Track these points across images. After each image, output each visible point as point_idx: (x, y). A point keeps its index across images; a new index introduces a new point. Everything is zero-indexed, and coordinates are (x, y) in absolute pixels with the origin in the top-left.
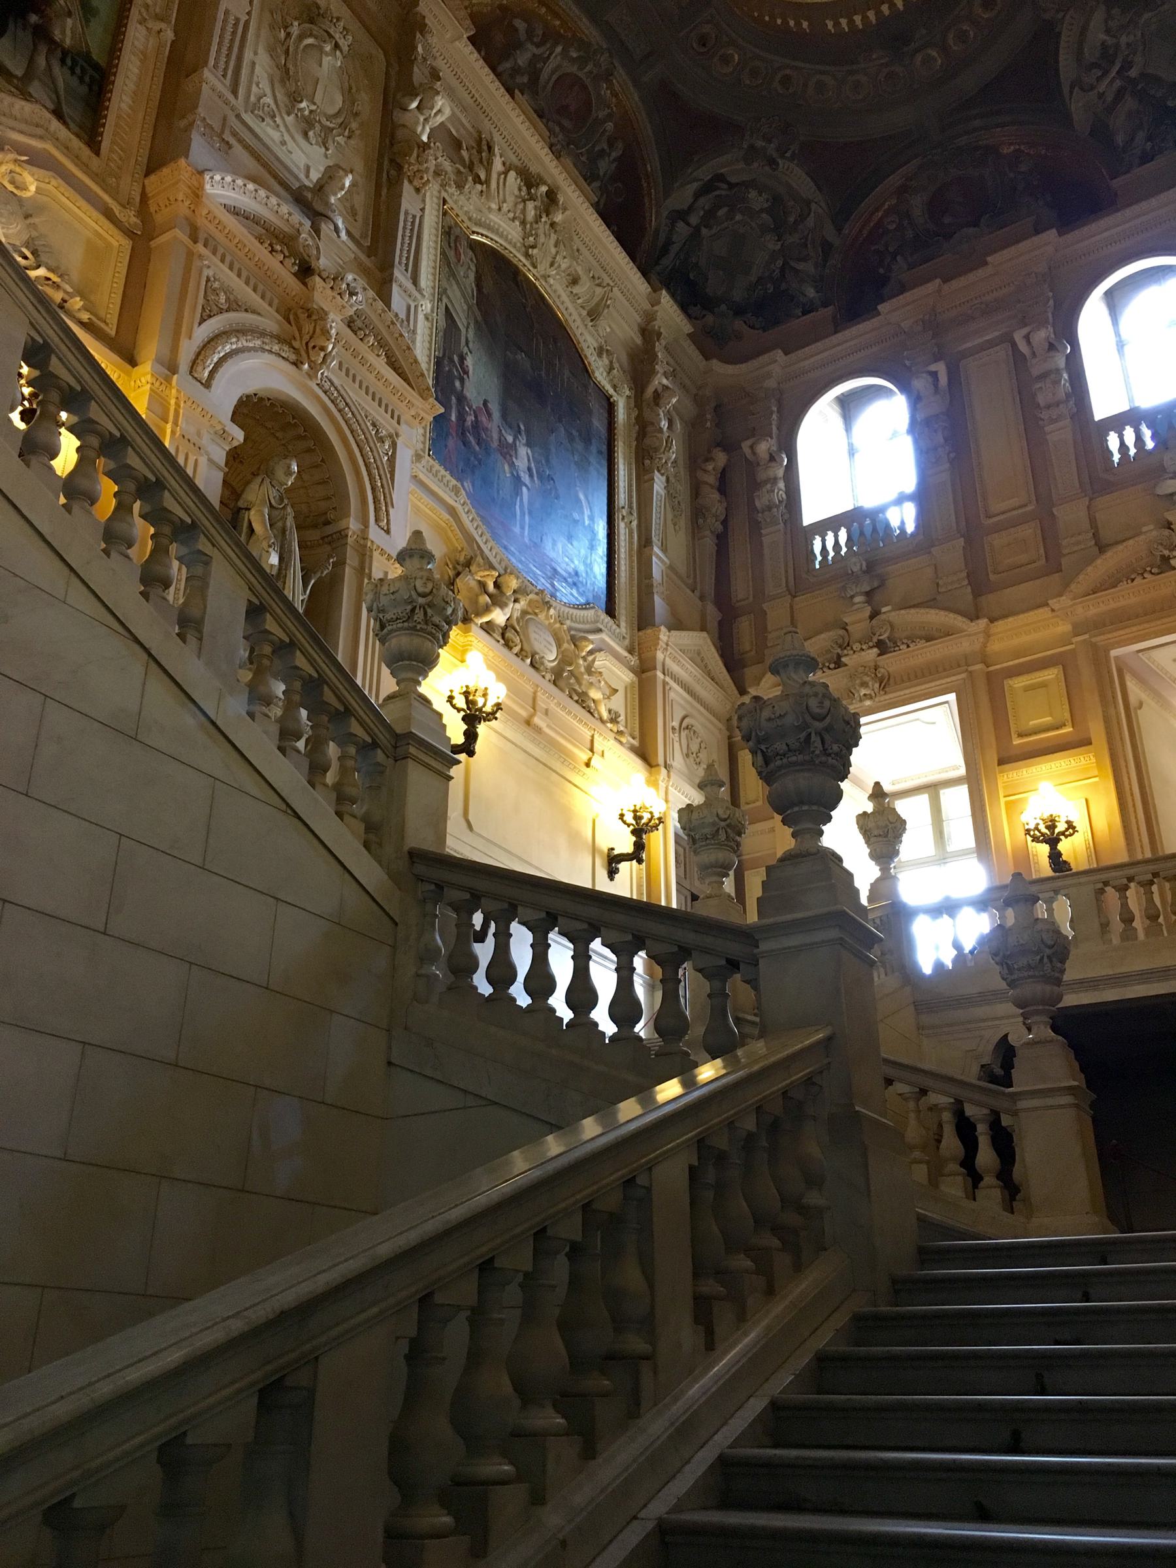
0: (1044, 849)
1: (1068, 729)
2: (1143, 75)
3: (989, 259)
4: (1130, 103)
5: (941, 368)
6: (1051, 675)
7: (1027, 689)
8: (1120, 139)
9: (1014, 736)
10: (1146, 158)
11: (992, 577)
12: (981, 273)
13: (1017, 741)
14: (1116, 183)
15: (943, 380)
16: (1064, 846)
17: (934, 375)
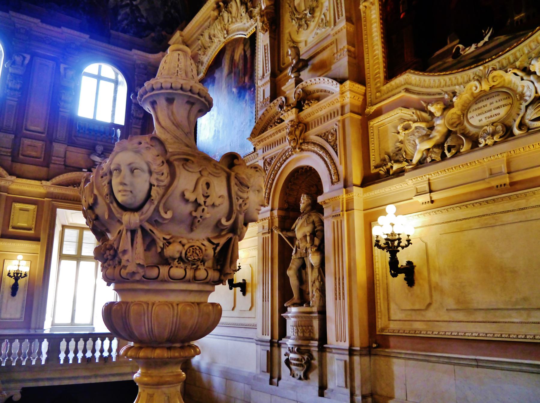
0: (13, 281)
1: (32, 232)
2: (136, 6)
3: (62, 28)
4: (128, 10)
5: (28, 57)
6: (32, 207)
7: (21, 209)
8: (119, 18)
9: (10, 227)
10: (124, 31)
11: (21, 157)
12: (56, 29)
13: (11, 230)
14: (113, 32)
15: (27, 62)
16: (19, 281)
17: (24, 58)
